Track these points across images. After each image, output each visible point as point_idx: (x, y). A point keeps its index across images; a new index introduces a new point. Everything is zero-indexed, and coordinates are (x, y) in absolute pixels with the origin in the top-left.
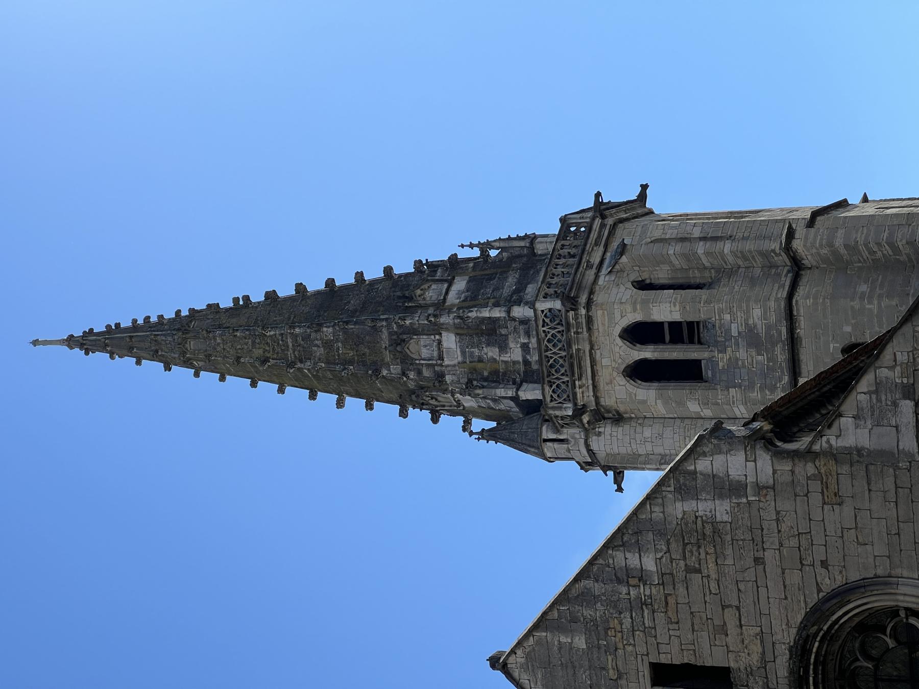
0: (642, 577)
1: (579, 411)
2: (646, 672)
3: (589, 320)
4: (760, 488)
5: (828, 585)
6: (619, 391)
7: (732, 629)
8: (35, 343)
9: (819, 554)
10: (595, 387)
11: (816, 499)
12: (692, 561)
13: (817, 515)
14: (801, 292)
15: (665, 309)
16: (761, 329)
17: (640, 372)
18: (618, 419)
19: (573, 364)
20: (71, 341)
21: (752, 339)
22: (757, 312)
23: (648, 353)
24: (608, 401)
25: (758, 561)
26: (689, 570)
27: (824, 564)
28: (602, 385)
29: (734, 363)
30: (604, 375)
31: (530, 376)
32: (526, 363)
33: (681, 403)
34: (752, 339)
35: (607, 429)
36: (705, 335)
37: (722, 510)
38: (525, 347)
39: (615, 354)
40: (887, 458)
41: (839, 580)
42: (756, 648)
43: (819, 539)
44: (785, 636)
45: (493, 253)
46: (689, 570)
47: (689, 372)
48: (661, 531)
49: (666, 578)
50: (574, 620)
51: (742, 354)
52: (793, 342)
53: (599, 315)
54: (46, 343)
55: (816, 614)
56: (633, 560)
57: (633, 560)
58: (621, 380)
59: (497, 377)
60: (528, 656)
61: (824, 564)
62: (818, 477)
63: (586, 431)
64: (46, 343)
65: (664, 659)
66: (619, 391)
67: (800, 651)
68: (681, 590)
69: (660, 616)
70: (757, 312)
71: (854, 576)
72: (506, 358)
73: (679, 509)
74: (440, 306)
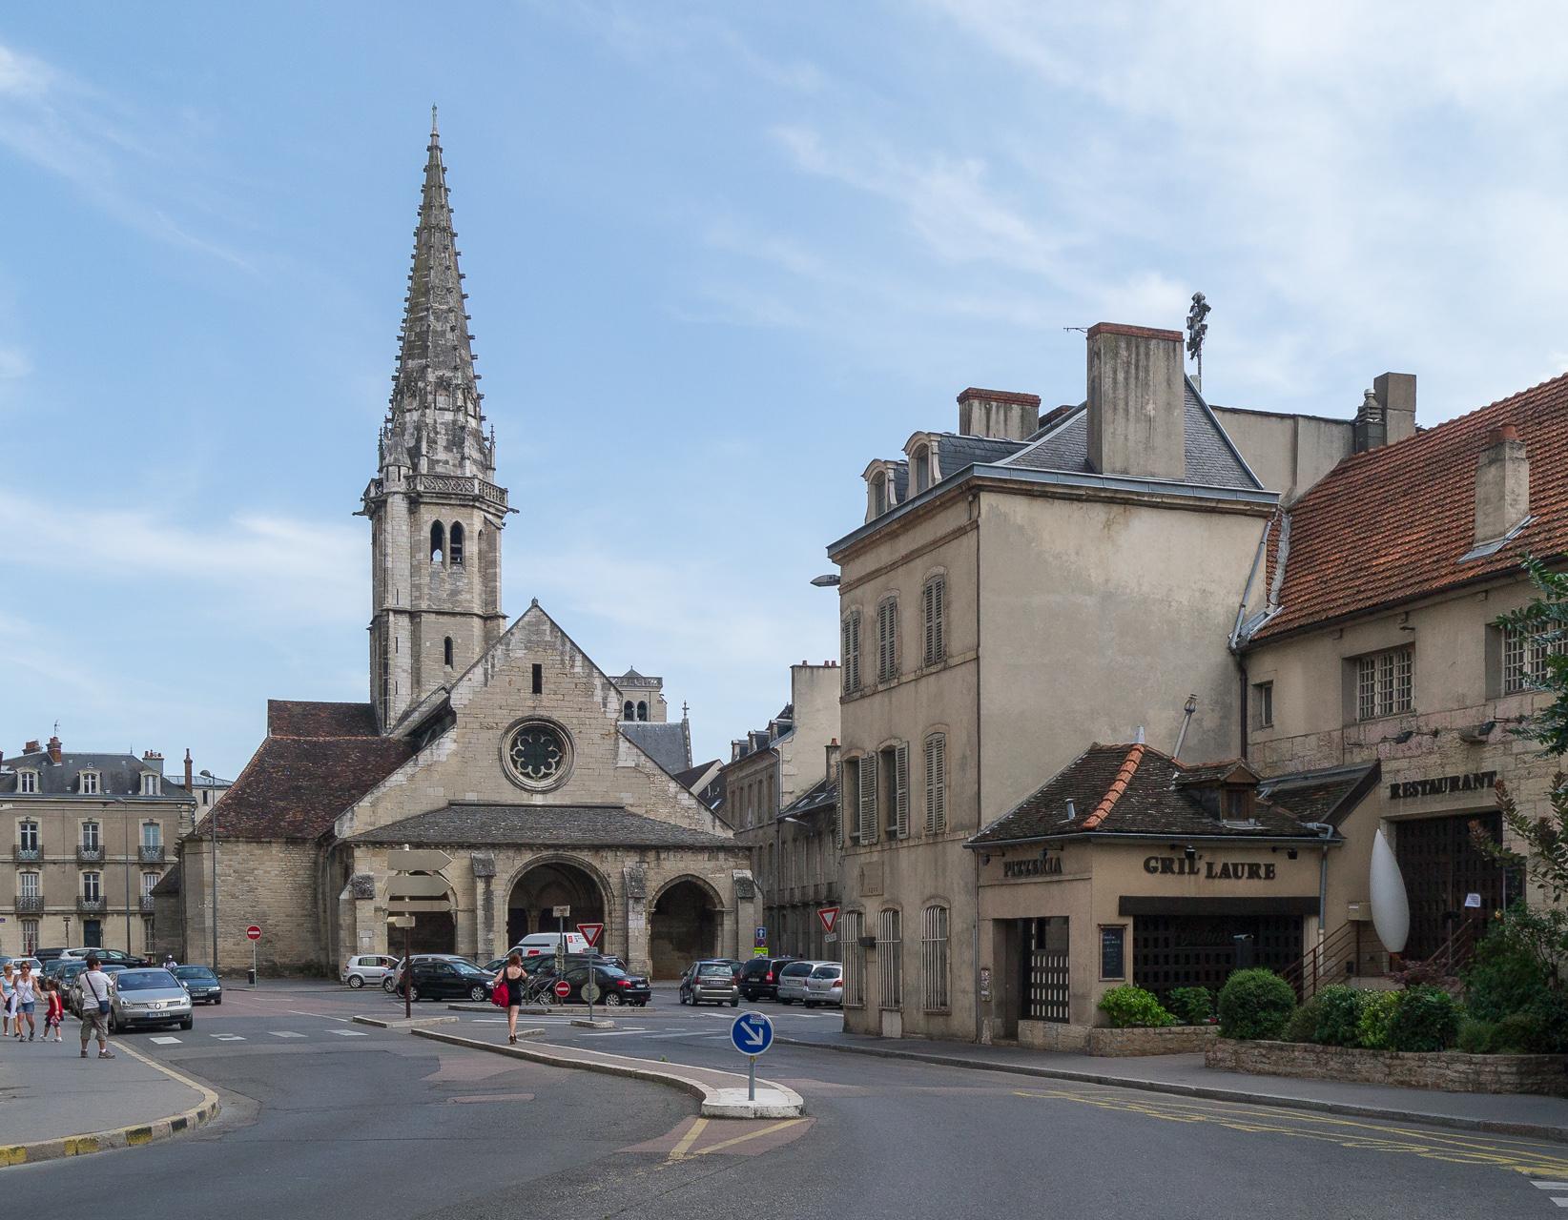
1: (419, 495)
6: (428, 516)
14: (476, 620)
15: (471, 548)
16: (460, 597)
17: (437, 529)
21: (454, 593)
23: (448, 535)
31: (432, 463)
34: (454, 593)
39: (448, 517)
44: (556, 716)
48: (590, 675)
52: (454, 614)
59: (432, 442)
72: (440, 449)
74: (467, 414)
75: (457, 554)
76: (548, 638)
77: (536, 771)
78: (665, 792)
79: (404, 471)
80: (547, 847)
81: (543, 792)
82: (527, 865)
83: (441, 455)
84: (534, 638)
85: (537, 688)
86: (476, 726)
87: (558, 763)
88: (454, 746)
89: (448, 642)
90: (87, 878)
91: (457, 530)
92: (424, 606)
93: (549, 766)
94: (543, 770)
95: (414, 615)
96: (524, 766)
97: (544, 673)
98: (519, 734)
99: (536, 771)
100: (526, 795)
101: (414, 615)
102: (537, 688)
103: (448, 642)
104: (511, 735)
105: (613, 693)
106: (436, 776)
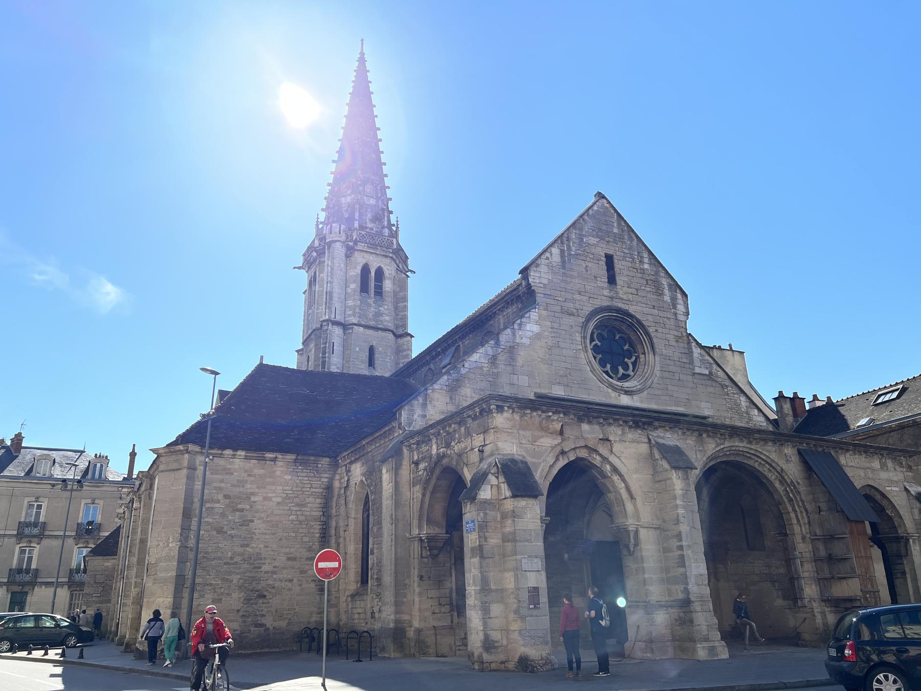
0: (641, 262)
2: (610, 252)
3: (386, 256)
4: (676, 314)
5: (651, 330)
7: (630, 290)
8: (362, 40)
9: (660, 330)
10: (362, 251)
11: (676, 333)
12: (650, 282)
13: (671, 332)
15: (388, 285)
16: (381, 318)
17: (365, 269)
18: (348, 256)
19: (374, 246)
20: (362, 54)
21: (378, 314)
22: (387, 318)
23: (373, 274)
24: (356, 254)
25: (654, 307)
26: (647, 280)
27: (656, 331)
28: (362, 254)
29: (369, 305)
30: (367, 256)
32: (367, 228)
33: (355, 282)
34: (378, 314)
35: (344, 250)
36: (378, 297)
37: (667, 298)
38: (372, 229)
39: (375, 263)
40: (691, 362)
41: (653, 335)
42: (625, 297)
43: (665, 331)
44: (632, 309)
45: (394, 228)
46: (647, 280)
47: (364, 288)
48: (657, 273)
49: (643, 271)
50: (623, 231)
51: (372, 309)
52: (376, 329)
53: (388, 261)
54: (362, 44)
55: (639, 321)
56: (646, 260)
57: (646, 260)
58: (364, 262)
60: (607, 208)
61: (656, 331)
62: (682, 336)
63: (343, 242)
64: (362, 44)
65: (616, 261)
66: (360, 259)
67: (627, 314)
68: (640, 275)
69: (630, 264)
70: (387, 318)
71: (655, 340)
73: (665, 282)
75: (379, 291)
76: (615, 230)
77: (615, 370)
78: (739, 405)
79: (343, 227)
80: (734, 432)
81: (628, 392)
82: (711, 458)
83: (369, 225)
84: (604, 227)
85: (612, 280)
86: (558, 308)
87: (634, 364)
88: (536, 329)
89: (372, 350)
90: (22, 552)
91: (380, 273)
92: (355, 321)
93: (626, 368)
94: (621, 371)
95: (345, 326)
96: (602, 363)
97: (618, 265)
98: (596, 327)
99: (615, 370)
100: (613, 394)
101: (345, 326)
102: (612, 280)
103: (372, 350)
104: (591, 326)
105: (679, 296)
106: (520, 361)
